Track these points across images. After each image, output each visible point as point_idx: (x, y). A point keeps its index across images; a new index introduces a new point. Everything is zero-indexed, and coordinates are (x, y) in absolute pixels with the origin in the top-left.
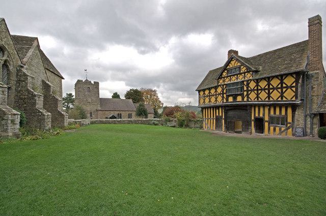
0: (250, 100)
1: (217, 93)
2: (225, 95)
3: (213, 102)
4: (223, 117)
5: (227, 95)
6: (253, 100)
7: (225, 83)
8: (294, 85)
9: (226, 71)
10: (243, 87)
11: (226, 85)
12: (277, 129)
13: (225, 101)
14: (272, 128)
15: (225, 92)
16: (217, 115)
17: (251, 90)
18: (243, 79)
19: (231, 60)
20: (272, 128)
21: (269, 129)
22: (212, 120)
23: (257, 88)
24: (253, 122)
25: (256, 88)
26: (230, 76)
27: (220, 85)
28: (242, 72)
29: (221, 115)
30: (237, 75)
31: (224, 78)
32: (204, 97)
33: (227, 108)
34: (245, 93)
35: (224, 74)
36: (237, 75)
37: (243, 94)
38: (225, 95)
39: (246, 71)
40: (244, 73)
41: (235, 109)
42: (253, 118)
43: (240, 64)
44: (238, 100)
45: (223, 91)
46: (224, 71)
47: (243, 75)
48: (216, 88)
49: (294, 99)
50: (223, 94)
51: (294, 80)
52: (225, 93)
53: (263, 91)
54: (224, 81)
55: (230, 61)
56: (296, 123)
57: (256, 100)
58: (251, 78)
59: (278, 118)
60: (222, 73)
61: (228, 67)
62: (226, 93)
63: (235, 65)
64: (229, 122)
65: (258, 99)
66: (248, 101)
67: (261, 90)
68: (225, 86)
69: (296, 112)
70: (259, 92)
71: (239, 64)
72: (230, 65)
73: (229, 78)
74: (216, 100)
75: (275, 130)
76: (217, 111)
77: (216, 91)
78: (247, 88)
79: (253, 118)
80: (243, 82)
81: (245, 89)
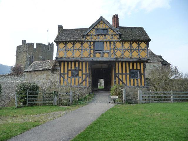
2: (92, 51)
7: (93, 40)
13: (92, 56)
15: (92, 47)
27: (87, 42)
30: (105, 35)
34: (112, 51)
35: (91, 32)
40: (112, 35)
43: (108, 27)
45: (90, 47)
47: (111, 36)
48: (82, 43)
50: (91, 49)
52: (92, 49)
53: (127, 51)
58: (118, 40)
61: (96, 27)
68: (92, 43)
71: (107, 27)
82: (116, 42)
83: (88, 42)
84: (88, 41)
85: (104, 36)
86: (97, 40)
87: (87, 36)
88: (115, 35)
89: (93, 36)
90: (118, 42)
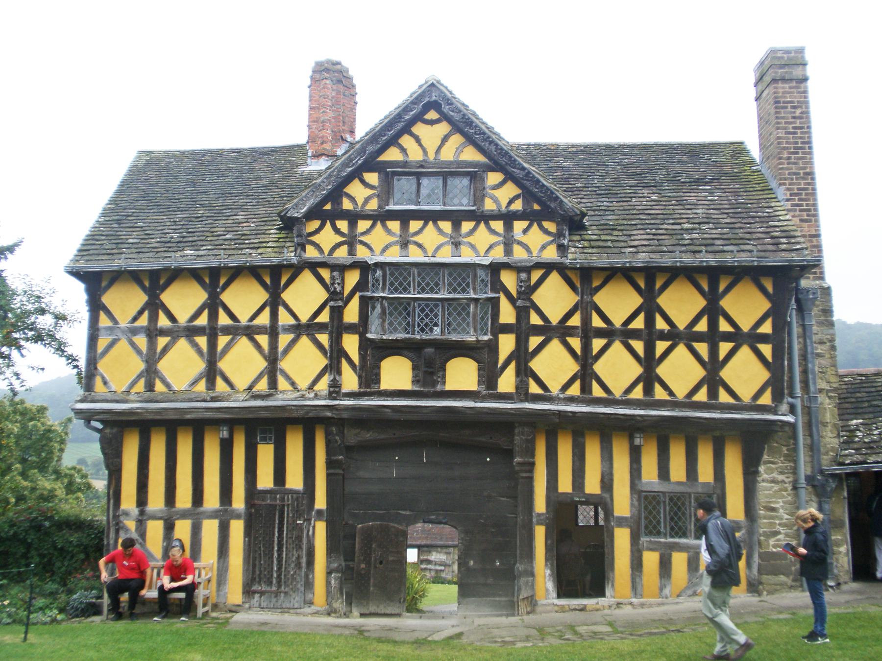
0: (534, 388)
1: (285, 318)
2: (351, 344)
3: (241, 383)
4: (321, 502)
5: (365, 345)
6: (555, 388)
7: (362, 253)
8: (766, 328)
9: (372, 178)
10: (495, 304)
11: (364, 267)
12: (679, 560)
13: (350, 381)
14: (651, 559)
15: (351, 314)
16: (265, 480)
17: (548, 331)
18: (498, 254)
19: (419, 118)
20: (651, 559)
21: (637, 564)
22: (210, 529)
23: (586, 320)
24: (540, 532)
25: (575, 321)
26: (404, 217)
27: (313, 266)
28: (489, 205)
29: (295, 480)
31: (353, 218)
32: (153, 333)
33: (353, 436)
34: (507, 344)
35: (356, 189)
36: (456, 218)
37: (493, 347)
38: (351, 344)
39: (518, 206)
40: (508, 218)
41: (418, 444)
42: (540, 505)
43: (479, 158)
44: (449, 387)
45: (337, 313)
46: (357, 174)
47: (498, 226)
49: (766, 399)
51: (766, 305)
52: (351, 328)
54: (351, 242)
55: (407, 129)
56: (763, 526)
57: (575, 390)
58: (551, 254)
59: (677, 502)
60: (348, 180)
61: (392, 155)
62: (360, 329)
63: (448, 154)
64: (368, 537)
65: (586, 388)
66: (522, 393)
67: (609, 333)
68: (352, 278)
69: (762, 469)
70: (597, 344)
71: (471, 155)
72: (406, 141)
73: (394, 226)
74: (272, 371)
75: (665, 566)
76: (266, 454)
77: (275, 302)
78: (522, 313)
79: (540, 505)
80: (495, 269)
81: (507, 314)
82: (536, 275)
83: (325, 274)
84: (324, 265)
85: (446, 226)
86: (394, 256)
87: (315, 224)
88: (532, 217)
89: (363, 225)
90: (554, 278)
